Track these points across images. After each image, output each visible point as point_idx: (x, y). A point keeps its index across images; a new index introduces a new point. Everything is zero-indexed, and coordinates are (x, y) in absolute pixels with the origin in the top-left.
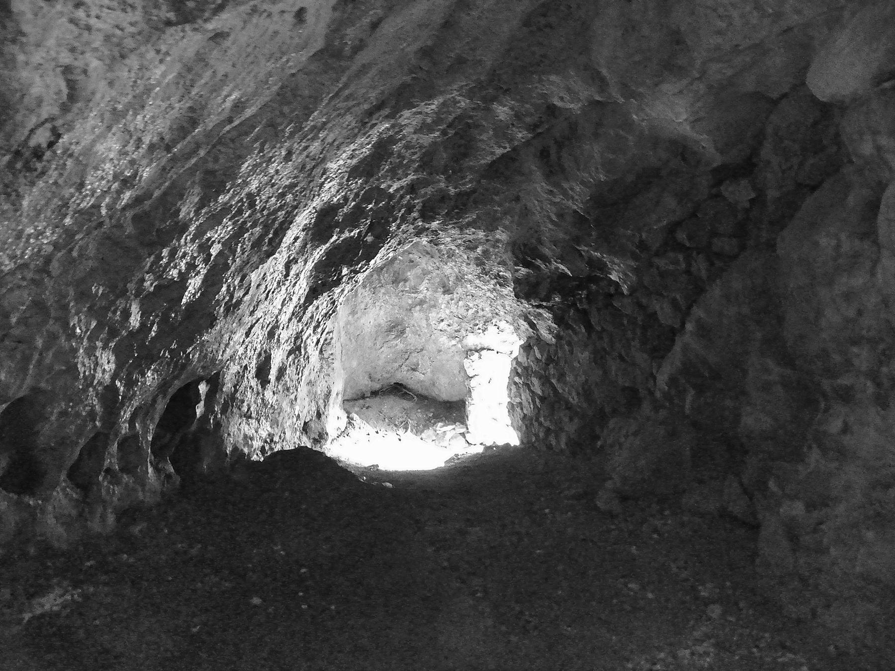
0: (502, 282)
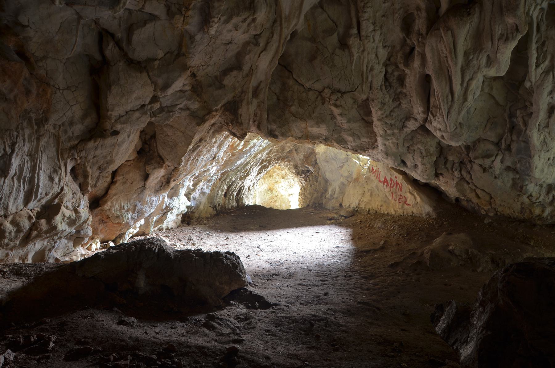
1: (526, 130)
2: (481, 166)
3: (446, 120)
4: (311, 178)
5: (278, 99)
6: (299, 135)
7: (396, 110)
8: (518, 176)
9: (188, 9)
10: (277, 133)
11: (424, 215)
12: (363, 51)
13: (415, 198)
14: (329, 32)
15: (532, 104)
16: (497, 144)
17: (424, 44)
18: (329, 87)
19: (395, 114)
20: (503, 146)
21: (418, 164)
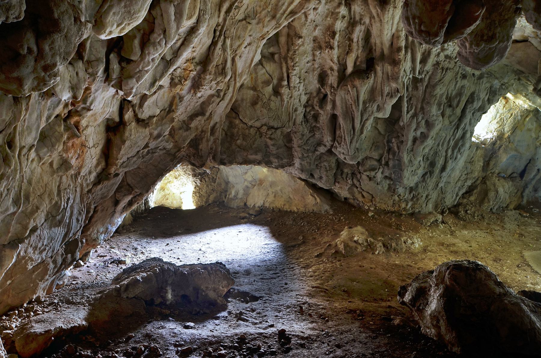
0: (189, 175)
1: (399, 152)
2: (368, 176)
3: (348, 147)
4: (207, 179)
5: (226, 134)
6: (241, 161)
7: (311, 139)
8: (392, 183)
9: (186, 80)
10: (226, 161)
11: (323, 212)
12: (291, 97)
13: (316, 199)
14: (267, 83)
15: (403, 136)
16: (379, 161)
17: (335, 95)
18: (265, 125)
19: (310, 142)
20: (383, 162)
21: (323, 176)
